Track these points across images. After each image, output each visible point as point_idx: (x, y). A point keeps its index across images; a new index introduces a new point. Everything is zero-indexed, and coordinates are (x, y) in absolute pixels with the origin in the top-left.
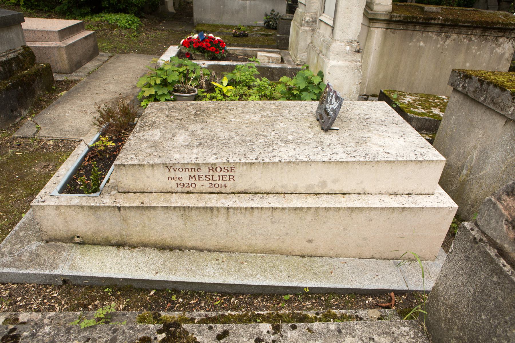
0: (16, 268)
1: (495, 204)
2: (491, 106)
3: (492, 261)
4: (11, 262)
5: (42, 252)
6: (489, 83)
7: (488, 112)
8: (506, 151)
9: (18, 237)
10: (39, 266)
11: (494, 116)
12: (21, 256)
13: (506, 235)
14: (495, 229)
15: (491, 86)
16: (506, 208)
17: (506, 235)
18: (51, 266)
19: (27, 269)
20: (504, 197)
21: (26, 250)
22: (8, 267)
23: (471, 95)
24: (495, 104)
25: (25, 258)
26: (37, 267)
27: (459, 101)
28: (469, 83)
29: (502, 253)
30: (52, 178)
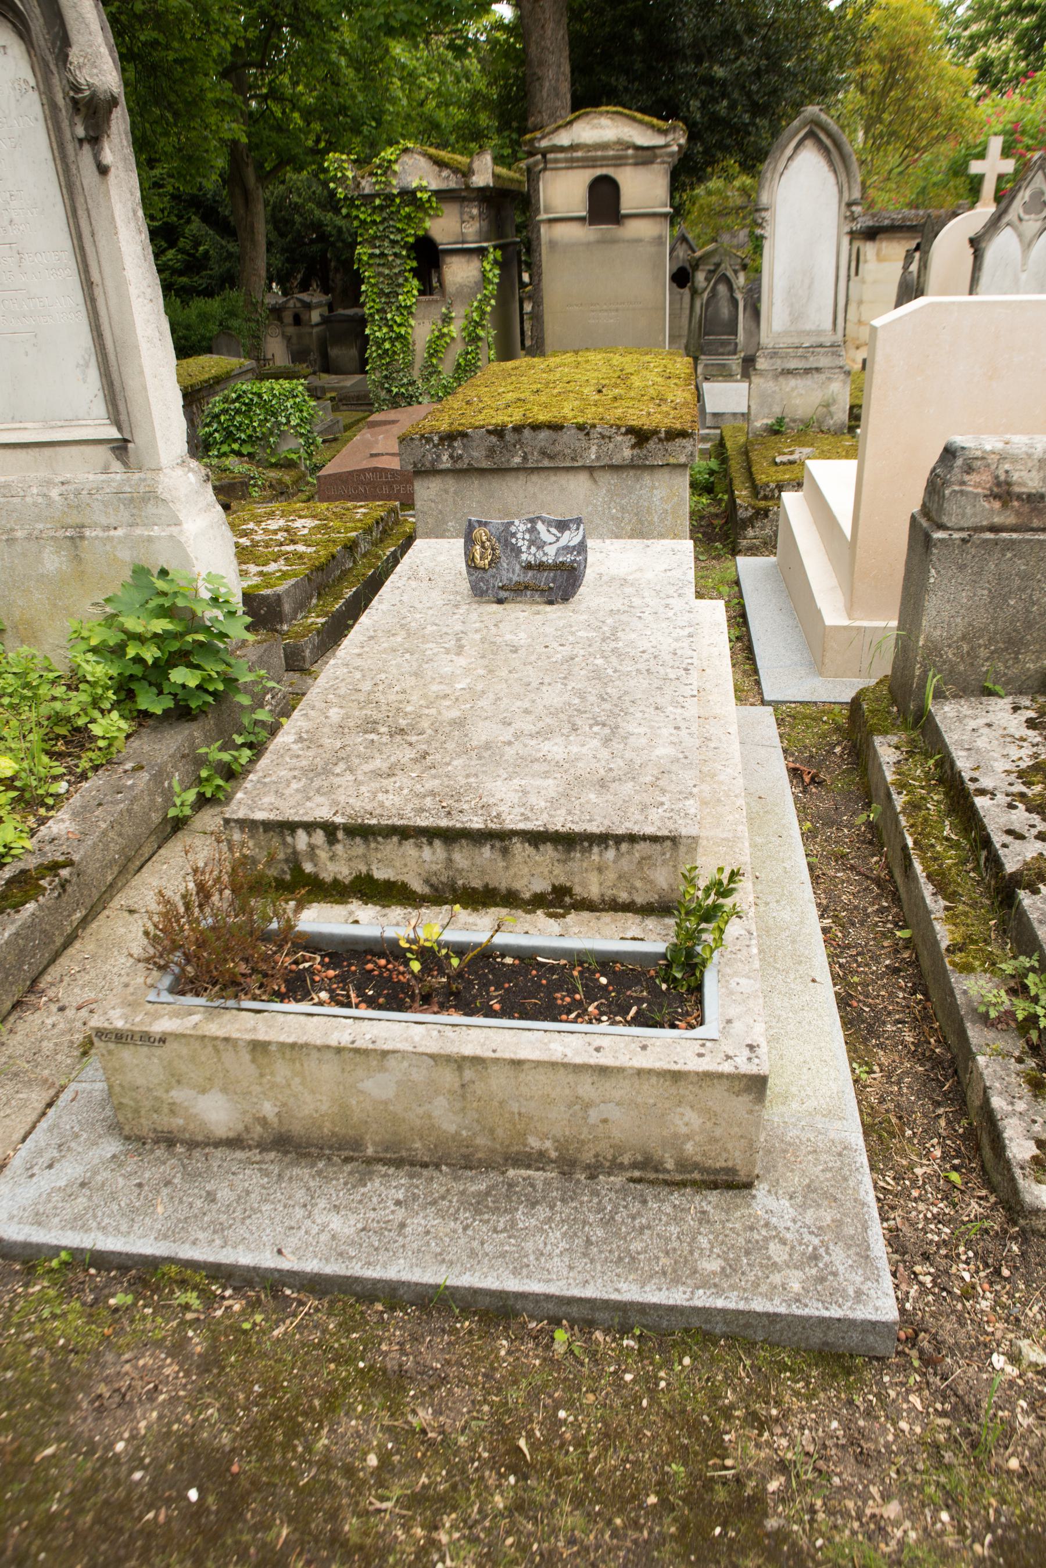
0: (865, 1228)
1: (962, 492)
2: (546, 463)
3: (996, 542)
4: (849, 1247)
5: (795, 1181)
6: (518, 429)
7: (535, 478)
8: (613, 518)
9: (731, 1269)
10: (845, 1179)
11: (553, 478)
12: (820, 1228)
13: (992, 510)
14: (975, 515)
15: (527, 432)
16: (975, 486)
17: (992, 510)
18: (840, 1155)
19: (864, 1204)
20: (966, 478)
21: (794, 1221)
22: (868, 1248)
23: (485, 464)
24: (551, 458)
25: (828, 1216)
26: (851, 1184)
27: (446, 492)
28: (465, 447)
29: (994, 529)
30: (814, 912)
